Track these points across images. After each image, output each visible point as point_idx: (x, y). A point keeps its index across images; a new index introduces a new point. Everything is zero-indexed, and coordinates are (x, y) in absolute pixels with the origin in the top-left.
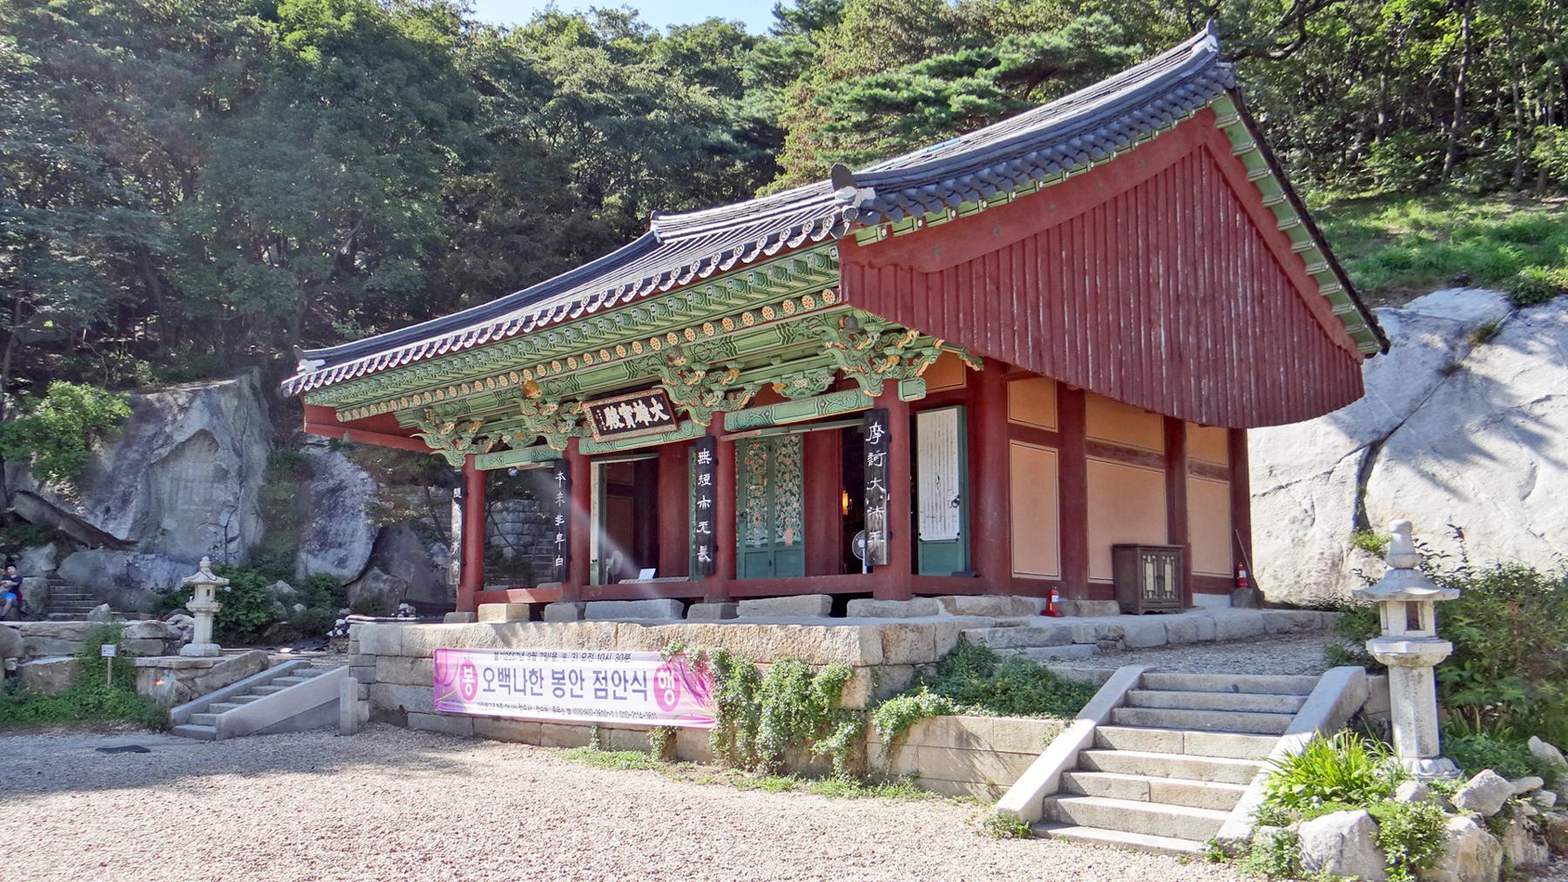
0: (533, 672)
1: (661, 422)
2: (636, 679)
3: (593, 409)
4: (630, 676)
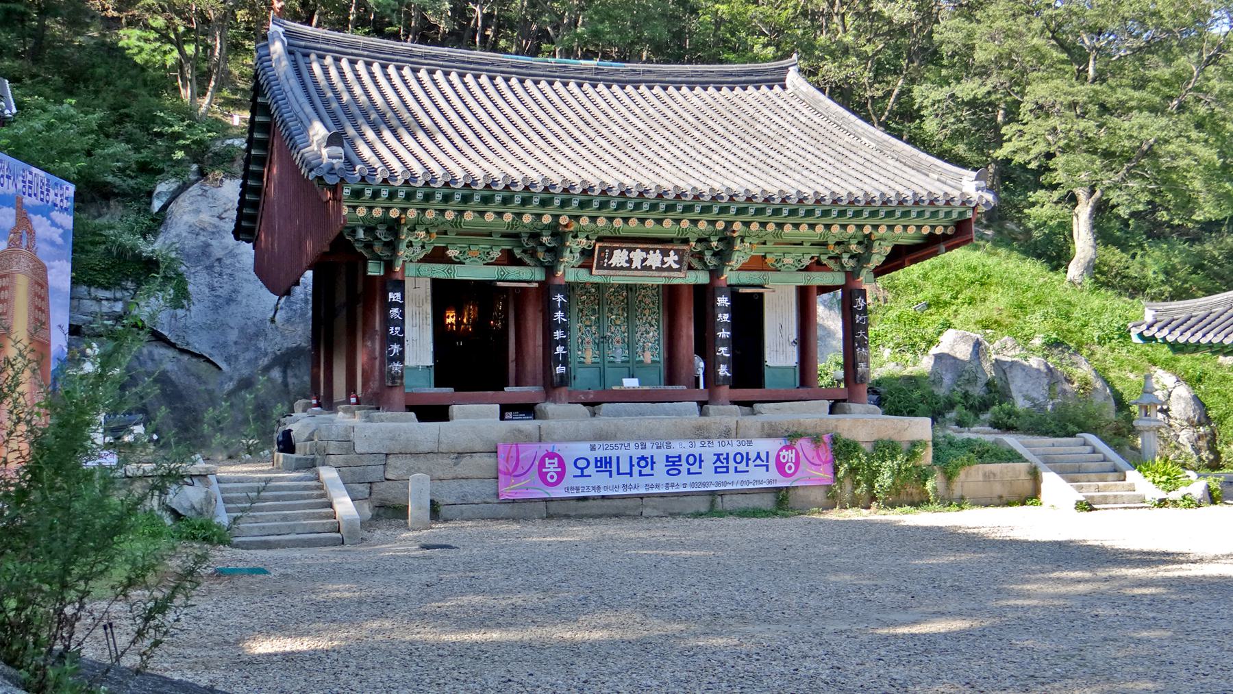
0: (643, 458)
1: (670, 269)
2: (758, 456)
3: (602, 249)
4: (753, 456)
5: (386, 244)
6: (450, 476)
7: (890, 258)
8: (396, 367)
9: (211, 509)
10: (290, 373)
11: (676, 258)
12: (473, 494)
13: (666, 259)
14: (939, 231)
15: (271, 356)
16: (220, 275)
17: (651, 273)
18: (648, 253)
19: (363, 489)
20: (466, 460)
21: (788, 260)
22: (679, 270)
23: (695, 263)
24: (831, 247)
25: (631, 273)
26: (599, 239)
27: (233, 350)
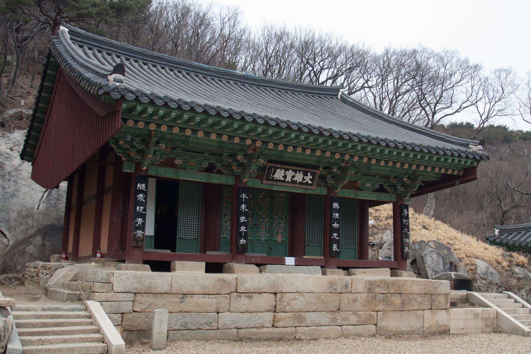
1: (307, 183)
5: (139, 151)
6: (178, 310)
7: (420, 187)
8: (139, 233)
9: (7, 335)
10: (47, 238)
11: (311, 177)
12: (192, 323)
13: (305, 177)
14: (456, 173)
15: (35, 229)
16: (9, 180)
18: (296, 173)
19: (118, 317)
20: (188, 299)
21: (368, 185)
24: (392, 179)
25: (285, 184)
26: (270, 161)
27: (13, 224)
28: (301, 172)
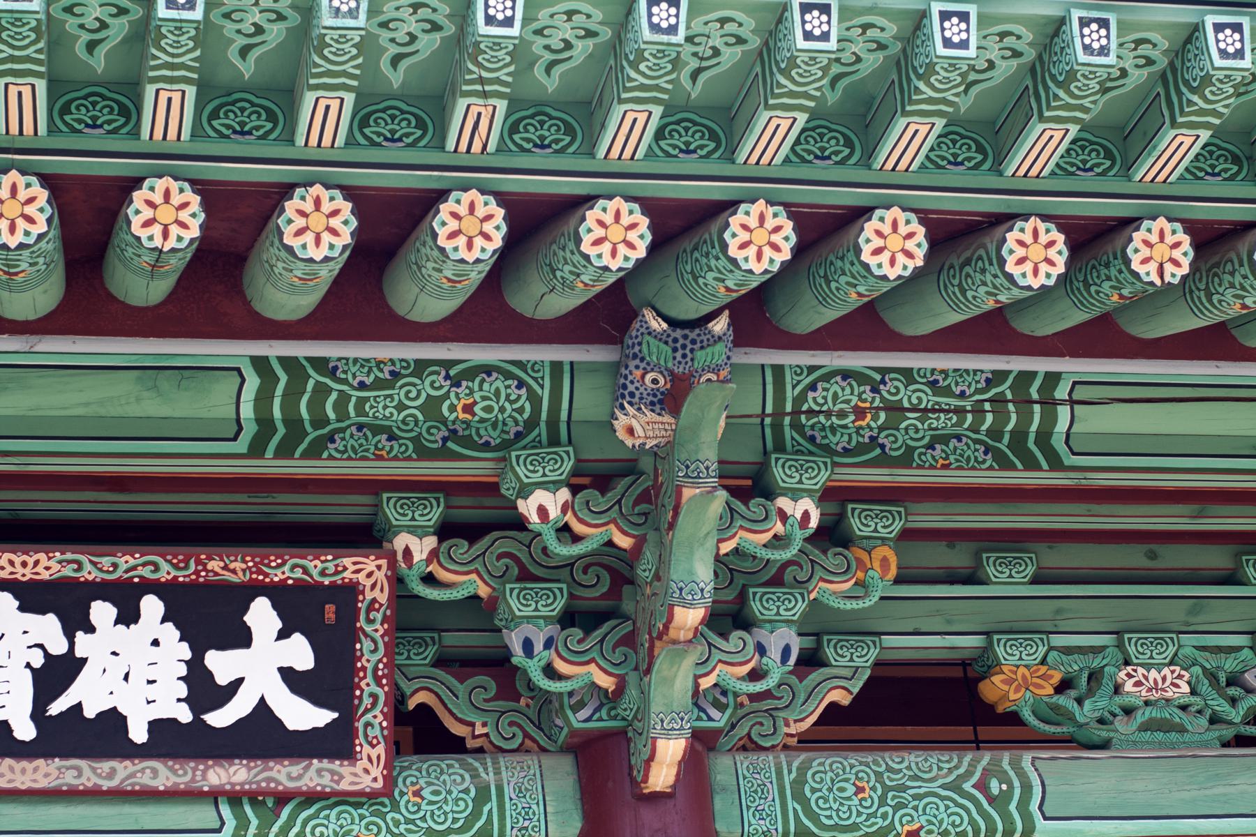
1: (262, 735)
13: (222, 665)
17: (120, 772)
18: (76, 622)
21: (1155, 679)
22: (334, 743)
23: (464, 707)
28: (152, 606)
